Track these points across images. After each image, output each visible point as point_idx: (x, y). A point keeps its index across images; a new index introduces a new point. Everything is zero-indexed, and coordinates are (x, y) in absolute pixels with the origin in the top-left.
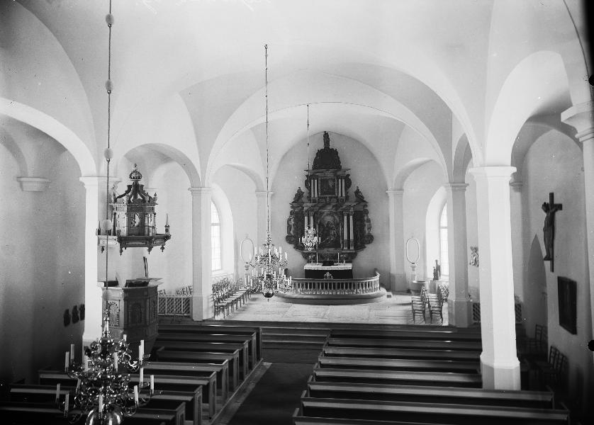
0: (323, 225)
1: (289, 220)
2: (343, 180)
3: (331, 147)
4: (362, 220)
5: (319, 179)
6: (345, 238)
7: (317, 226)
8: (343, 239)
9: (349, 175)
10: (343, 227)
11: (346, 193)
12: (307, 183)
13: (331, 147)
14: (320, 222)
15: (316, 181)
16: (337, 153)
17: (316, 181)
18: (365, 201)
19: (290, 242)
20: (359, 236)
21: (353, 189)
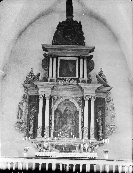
0: (60, 112)
1: (21, 103)
2: (85, 61)
3: (74, 19)
4: (104, 109)
5: (59, 58)
6: (86, 125)
7: (53, 112)
8: (83, 127)
9: (92, 56)
10: (83, 115)
11: (88, 76)
12: (45, 64)
13: (74, 19)
14: (57, 109)
15: (55, 60)
16: (81, 27)
17: (55, 60)
18: (108, 86)
19: (21, 130)
20: (100, 124)
21: (96, 71)
